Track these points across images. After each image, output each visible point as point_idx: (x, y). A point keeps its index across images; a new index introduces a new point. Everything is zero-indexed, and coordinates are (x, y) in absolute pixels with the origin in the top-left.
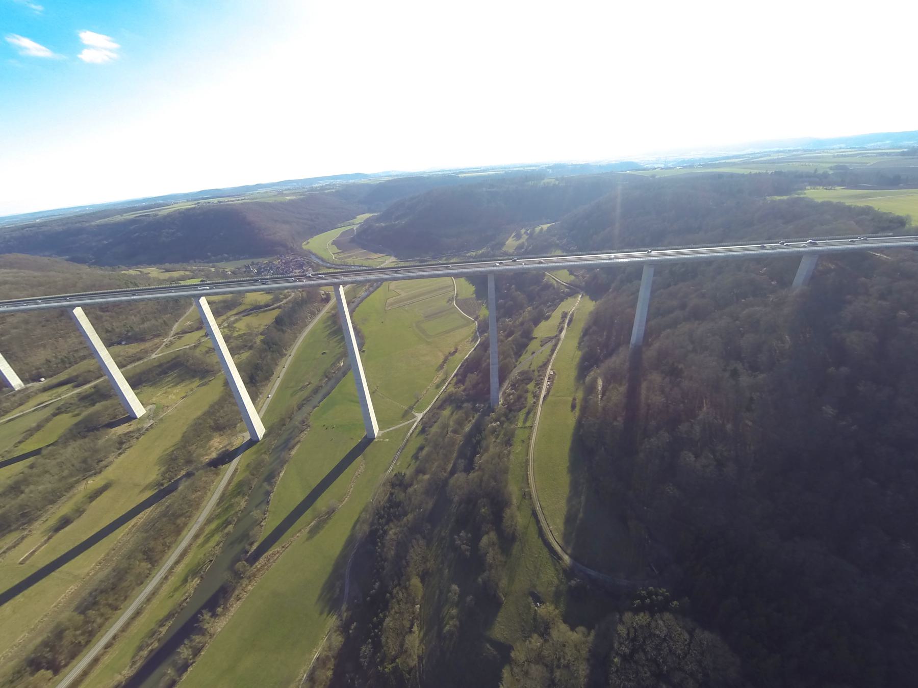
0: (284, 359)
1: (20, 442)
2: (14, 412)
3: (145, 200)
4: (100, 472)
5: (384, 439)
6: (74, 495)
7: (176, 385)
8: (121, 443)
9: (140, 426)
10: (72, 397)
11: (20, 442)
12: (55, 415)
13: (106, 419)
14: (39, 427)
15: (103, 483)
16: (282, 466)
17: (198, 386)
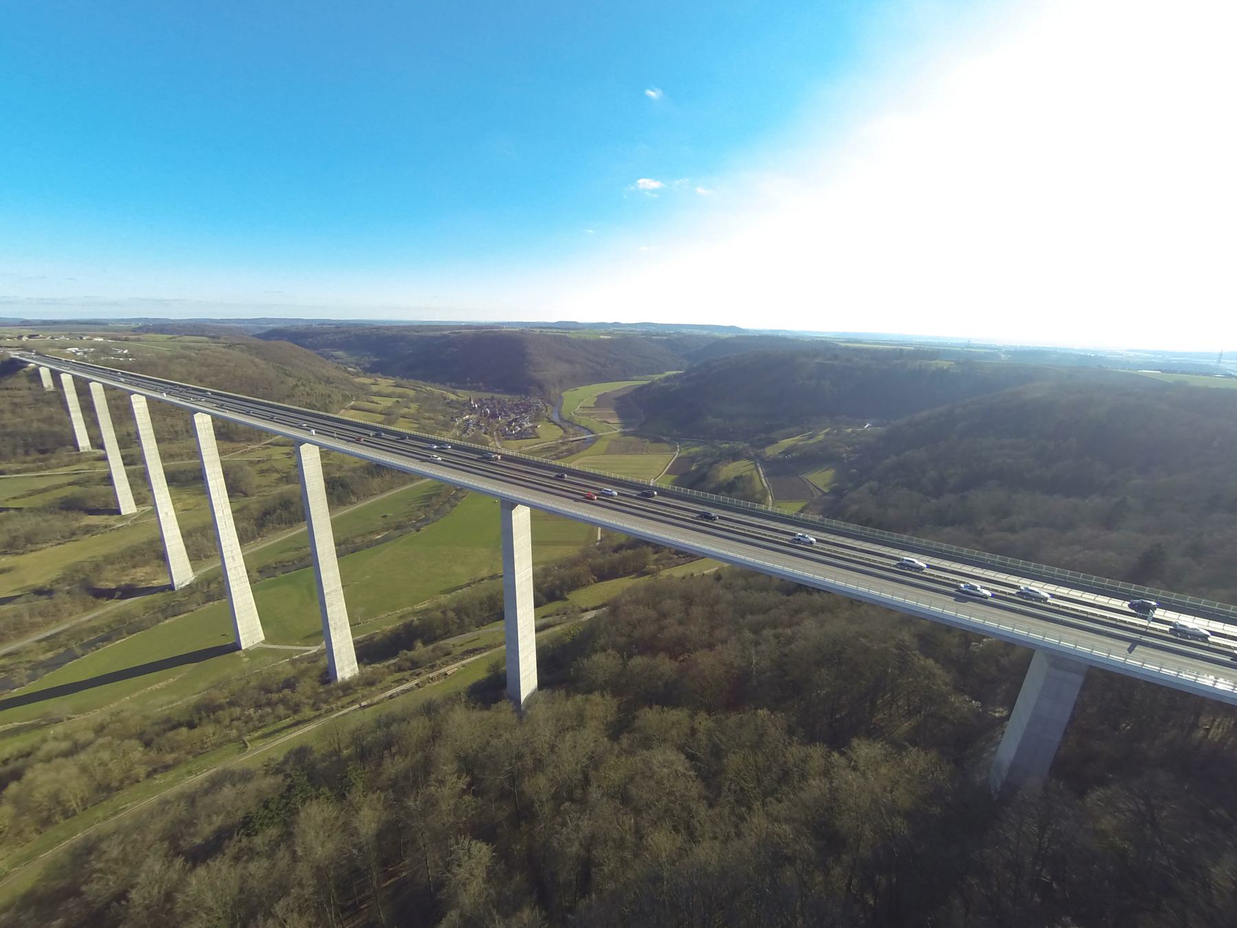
0: (341, 508)
1: (14, 498)
2: (57, 470)
3: (538, 323)
7: (200, 494)
8: (73, 534)
10: (99, 474)
11: (14, 498)
12: (69, 484)
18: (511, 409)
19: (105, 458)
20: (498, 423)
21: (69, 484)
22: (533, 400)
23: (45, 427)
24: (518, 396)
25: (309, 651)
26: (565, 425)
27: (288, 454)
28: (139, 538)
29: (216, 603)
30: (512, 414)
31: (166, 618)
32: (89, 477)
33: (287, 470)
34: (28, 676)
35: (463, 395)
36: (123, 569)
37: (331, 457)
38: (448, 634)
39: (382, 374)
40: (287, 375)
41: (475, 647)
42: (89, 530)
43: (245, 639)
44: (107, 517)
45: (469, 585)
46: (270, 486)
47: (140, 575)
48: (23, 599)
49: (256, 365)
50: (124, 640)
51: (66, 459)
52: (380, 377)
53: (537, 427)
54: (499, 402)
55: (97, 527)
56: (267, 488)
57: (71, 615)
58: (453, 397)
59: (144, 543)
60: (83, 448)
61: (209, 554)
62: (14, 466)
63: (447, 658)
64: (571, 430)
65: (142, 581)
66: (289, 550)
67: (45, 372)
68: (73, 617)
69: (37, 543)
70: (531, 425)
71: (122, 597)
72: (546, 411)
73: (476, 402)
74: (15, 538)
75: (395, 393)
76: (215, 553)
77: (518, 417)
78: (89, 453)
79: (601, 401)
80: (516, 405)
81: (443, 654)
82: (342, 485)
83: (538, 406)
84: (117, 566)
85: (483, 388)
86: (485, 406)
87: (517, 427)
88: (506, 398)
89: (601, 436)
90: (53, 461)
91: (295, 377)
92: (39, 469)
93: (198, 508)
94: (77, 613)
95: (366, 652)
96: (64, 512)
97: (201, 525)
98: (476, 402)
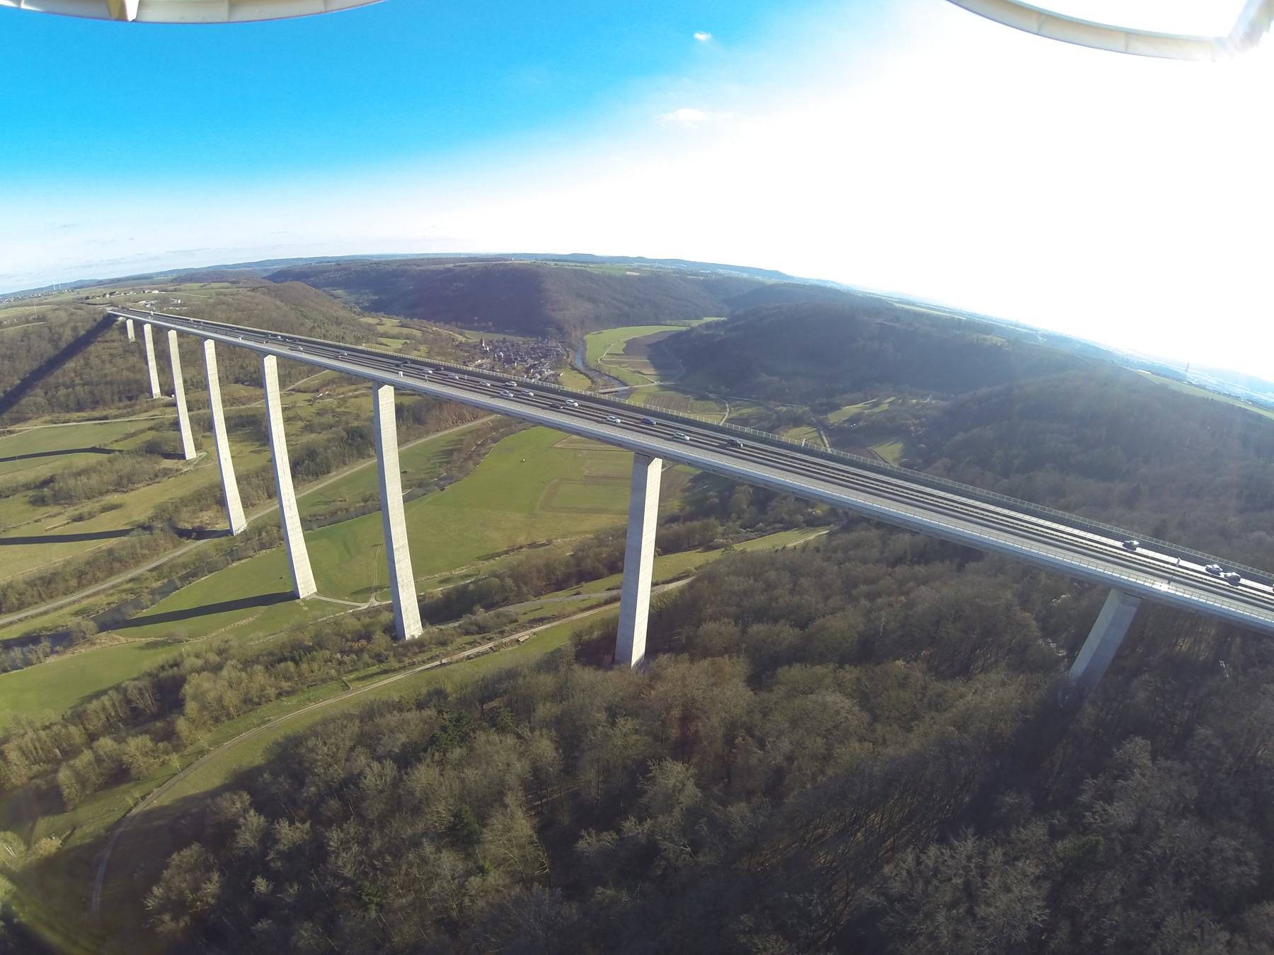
1: (116, 441)
4: (127, 492)
5: (305, 605)
6: (102, 500)
7: (240, 441)
8: (156, 476)
9: (181, 467)
11: (116, 441)
12: (150, 429)
13: (168, 449)
14: (133, 435)
15: (119, 502)
16: (210, 572)
17: (251, 452)
18: (527, 353)
19: (174, 405)
20: (514, 369)
21: (150, 429)
22: (552, 343)
23: (131, 375)
24: (534, 339)
25: (359, 607)
26: (591, 374)
27: (310, 401)
28: (200, 482)
29: (268, 551)
30: (529, 360)
31: (233, 561)
32: (162, 423)
33: (310, 419)
34: (150, 600)
35: (472, 337)
36: (194, 512)
37: (348, 404)
38: (506, 601)
39: (385, 314)
40: (305, 316)
41: (542, 616)
42: (166, 473)
43: (302, 589)
44: (176, 461)
45: (507, 552)
46: (297, 435)
47: (206, 517)
48: (134, 533)
49: (279, 308)
50: (206, 577)
51: (145, 405)
52: (383, 317)
53: (559, 375)
54: (513, 345)
55: (171, 470)
56: (294, 437)
57: (165, 550)
58: (463, 339)
59: (206, 488)
60: (156, 395)
61: (253, 502)
62: (114, 412)
63: (513, 625)
64: (600, 381)
65: (208, 524)
66: (320, 503)
67: (130, 323)
68: (167, 552)
69: (134, 483)
70: (552, 372)
71: (198, 538)
72: (568, 357)
73: (487, 344)
74: (121, 477)
75: (401, 334)
76: (258, 502)
77: (536, 363)
78: (159, 399)
79: (632, 348)
80: (533, 349)
81: (508, 621)
82: (361, 436)
83: (557, 351)
84: (190, 508)
85: (493, 329)
86: (498, 350)
87: (537, 375)
88: (519, 340)
89: (636, 389)
90: (137, 407)
91: (312, 319)
92: (128, 415)
93: (240, 455)
94: (169, 549)
95: (429, 613)
96: (149, 455)
97: (245, 473)
98: (487, 344)
